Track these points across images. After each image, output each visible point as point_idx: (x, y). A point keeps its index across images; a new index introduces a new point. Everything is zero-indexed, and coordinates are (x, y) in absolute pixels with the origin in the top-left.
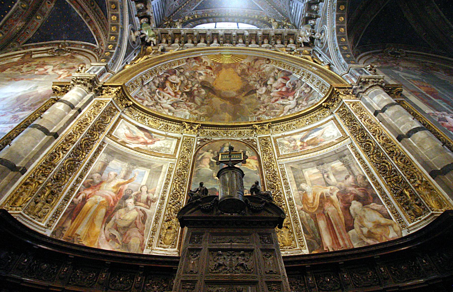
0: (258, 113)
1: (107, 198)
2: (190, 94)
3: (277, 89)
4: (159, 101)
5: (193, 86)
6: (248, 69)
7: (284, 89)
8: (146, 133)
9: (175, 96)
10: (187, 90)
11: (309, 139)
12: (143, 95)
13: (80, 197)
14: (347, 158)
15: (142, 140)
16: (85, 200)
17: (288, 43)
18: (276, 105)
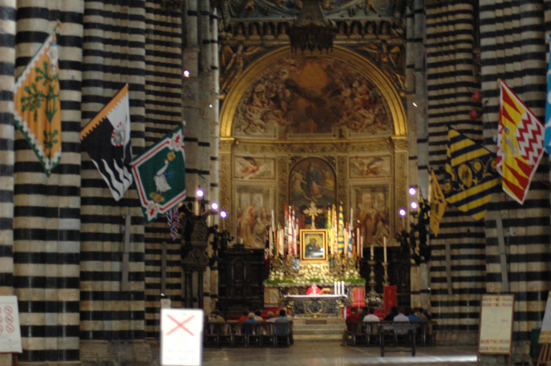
0: (342, 121)
1: (247, 220)
2: (276, 99)
3: (361, 95)
4: (251, 118)
5: (278, 88)
6: (334, 66)
7: (367, 98)
8: (252, 161)
9: (263, 106)
10: (273, 95)
11: (372, 166)
12: (240, 122)
13: (238, 224)
14: (387, 193)
15: (250, 169)
16: (240, 224)
17: (381, 33)
18: (358, 115)
